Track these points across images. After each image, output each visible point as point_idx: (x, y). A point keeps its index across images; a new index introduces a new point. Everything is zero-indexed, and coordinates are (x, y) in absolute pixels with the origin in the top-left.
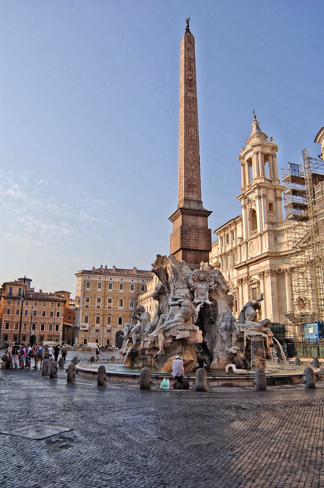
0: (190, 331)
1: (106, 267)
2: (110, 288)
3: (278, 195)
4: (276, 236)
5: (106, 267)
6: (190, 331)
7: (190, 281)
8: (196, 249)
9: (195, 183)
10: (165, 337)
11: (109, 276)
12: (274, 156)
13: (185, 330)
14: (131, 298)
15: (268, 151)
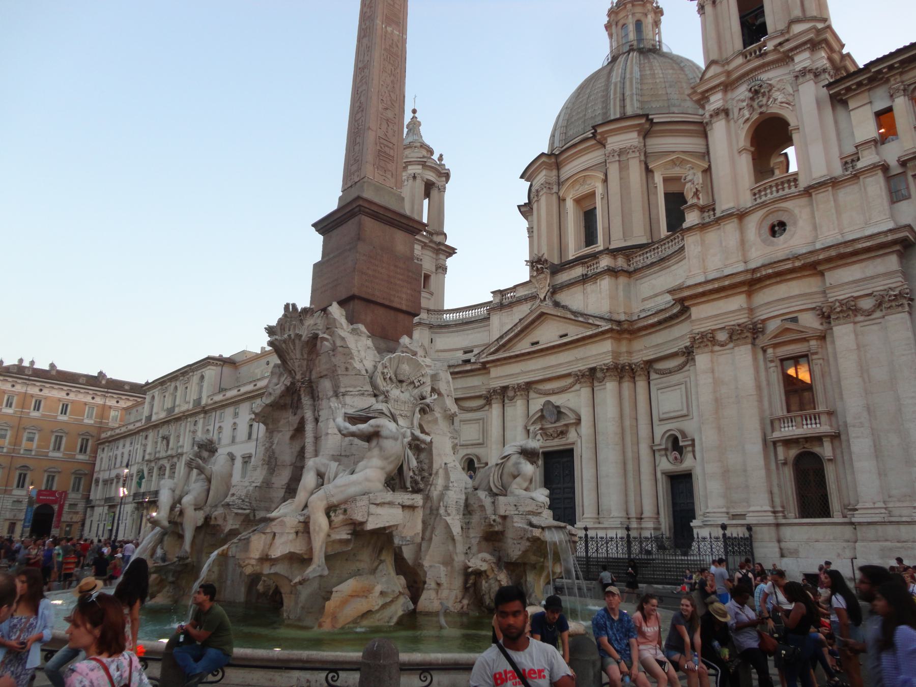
0: (404, 507)
1: (32, 363)
2: (37, 407)
3: (441, 262)
4: (433, 336)
5: (32, 363)
6: (404, 507)
7: (380, 381)
8: (387, 303)
9: (391, 153)
10: (330, 522)
11: (38, 384)
12: (442, 190)
13: (390, 504)
14: (82, 435)
15: (431, 176)
